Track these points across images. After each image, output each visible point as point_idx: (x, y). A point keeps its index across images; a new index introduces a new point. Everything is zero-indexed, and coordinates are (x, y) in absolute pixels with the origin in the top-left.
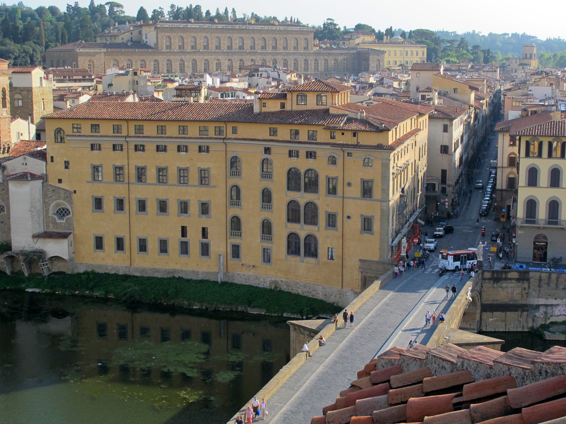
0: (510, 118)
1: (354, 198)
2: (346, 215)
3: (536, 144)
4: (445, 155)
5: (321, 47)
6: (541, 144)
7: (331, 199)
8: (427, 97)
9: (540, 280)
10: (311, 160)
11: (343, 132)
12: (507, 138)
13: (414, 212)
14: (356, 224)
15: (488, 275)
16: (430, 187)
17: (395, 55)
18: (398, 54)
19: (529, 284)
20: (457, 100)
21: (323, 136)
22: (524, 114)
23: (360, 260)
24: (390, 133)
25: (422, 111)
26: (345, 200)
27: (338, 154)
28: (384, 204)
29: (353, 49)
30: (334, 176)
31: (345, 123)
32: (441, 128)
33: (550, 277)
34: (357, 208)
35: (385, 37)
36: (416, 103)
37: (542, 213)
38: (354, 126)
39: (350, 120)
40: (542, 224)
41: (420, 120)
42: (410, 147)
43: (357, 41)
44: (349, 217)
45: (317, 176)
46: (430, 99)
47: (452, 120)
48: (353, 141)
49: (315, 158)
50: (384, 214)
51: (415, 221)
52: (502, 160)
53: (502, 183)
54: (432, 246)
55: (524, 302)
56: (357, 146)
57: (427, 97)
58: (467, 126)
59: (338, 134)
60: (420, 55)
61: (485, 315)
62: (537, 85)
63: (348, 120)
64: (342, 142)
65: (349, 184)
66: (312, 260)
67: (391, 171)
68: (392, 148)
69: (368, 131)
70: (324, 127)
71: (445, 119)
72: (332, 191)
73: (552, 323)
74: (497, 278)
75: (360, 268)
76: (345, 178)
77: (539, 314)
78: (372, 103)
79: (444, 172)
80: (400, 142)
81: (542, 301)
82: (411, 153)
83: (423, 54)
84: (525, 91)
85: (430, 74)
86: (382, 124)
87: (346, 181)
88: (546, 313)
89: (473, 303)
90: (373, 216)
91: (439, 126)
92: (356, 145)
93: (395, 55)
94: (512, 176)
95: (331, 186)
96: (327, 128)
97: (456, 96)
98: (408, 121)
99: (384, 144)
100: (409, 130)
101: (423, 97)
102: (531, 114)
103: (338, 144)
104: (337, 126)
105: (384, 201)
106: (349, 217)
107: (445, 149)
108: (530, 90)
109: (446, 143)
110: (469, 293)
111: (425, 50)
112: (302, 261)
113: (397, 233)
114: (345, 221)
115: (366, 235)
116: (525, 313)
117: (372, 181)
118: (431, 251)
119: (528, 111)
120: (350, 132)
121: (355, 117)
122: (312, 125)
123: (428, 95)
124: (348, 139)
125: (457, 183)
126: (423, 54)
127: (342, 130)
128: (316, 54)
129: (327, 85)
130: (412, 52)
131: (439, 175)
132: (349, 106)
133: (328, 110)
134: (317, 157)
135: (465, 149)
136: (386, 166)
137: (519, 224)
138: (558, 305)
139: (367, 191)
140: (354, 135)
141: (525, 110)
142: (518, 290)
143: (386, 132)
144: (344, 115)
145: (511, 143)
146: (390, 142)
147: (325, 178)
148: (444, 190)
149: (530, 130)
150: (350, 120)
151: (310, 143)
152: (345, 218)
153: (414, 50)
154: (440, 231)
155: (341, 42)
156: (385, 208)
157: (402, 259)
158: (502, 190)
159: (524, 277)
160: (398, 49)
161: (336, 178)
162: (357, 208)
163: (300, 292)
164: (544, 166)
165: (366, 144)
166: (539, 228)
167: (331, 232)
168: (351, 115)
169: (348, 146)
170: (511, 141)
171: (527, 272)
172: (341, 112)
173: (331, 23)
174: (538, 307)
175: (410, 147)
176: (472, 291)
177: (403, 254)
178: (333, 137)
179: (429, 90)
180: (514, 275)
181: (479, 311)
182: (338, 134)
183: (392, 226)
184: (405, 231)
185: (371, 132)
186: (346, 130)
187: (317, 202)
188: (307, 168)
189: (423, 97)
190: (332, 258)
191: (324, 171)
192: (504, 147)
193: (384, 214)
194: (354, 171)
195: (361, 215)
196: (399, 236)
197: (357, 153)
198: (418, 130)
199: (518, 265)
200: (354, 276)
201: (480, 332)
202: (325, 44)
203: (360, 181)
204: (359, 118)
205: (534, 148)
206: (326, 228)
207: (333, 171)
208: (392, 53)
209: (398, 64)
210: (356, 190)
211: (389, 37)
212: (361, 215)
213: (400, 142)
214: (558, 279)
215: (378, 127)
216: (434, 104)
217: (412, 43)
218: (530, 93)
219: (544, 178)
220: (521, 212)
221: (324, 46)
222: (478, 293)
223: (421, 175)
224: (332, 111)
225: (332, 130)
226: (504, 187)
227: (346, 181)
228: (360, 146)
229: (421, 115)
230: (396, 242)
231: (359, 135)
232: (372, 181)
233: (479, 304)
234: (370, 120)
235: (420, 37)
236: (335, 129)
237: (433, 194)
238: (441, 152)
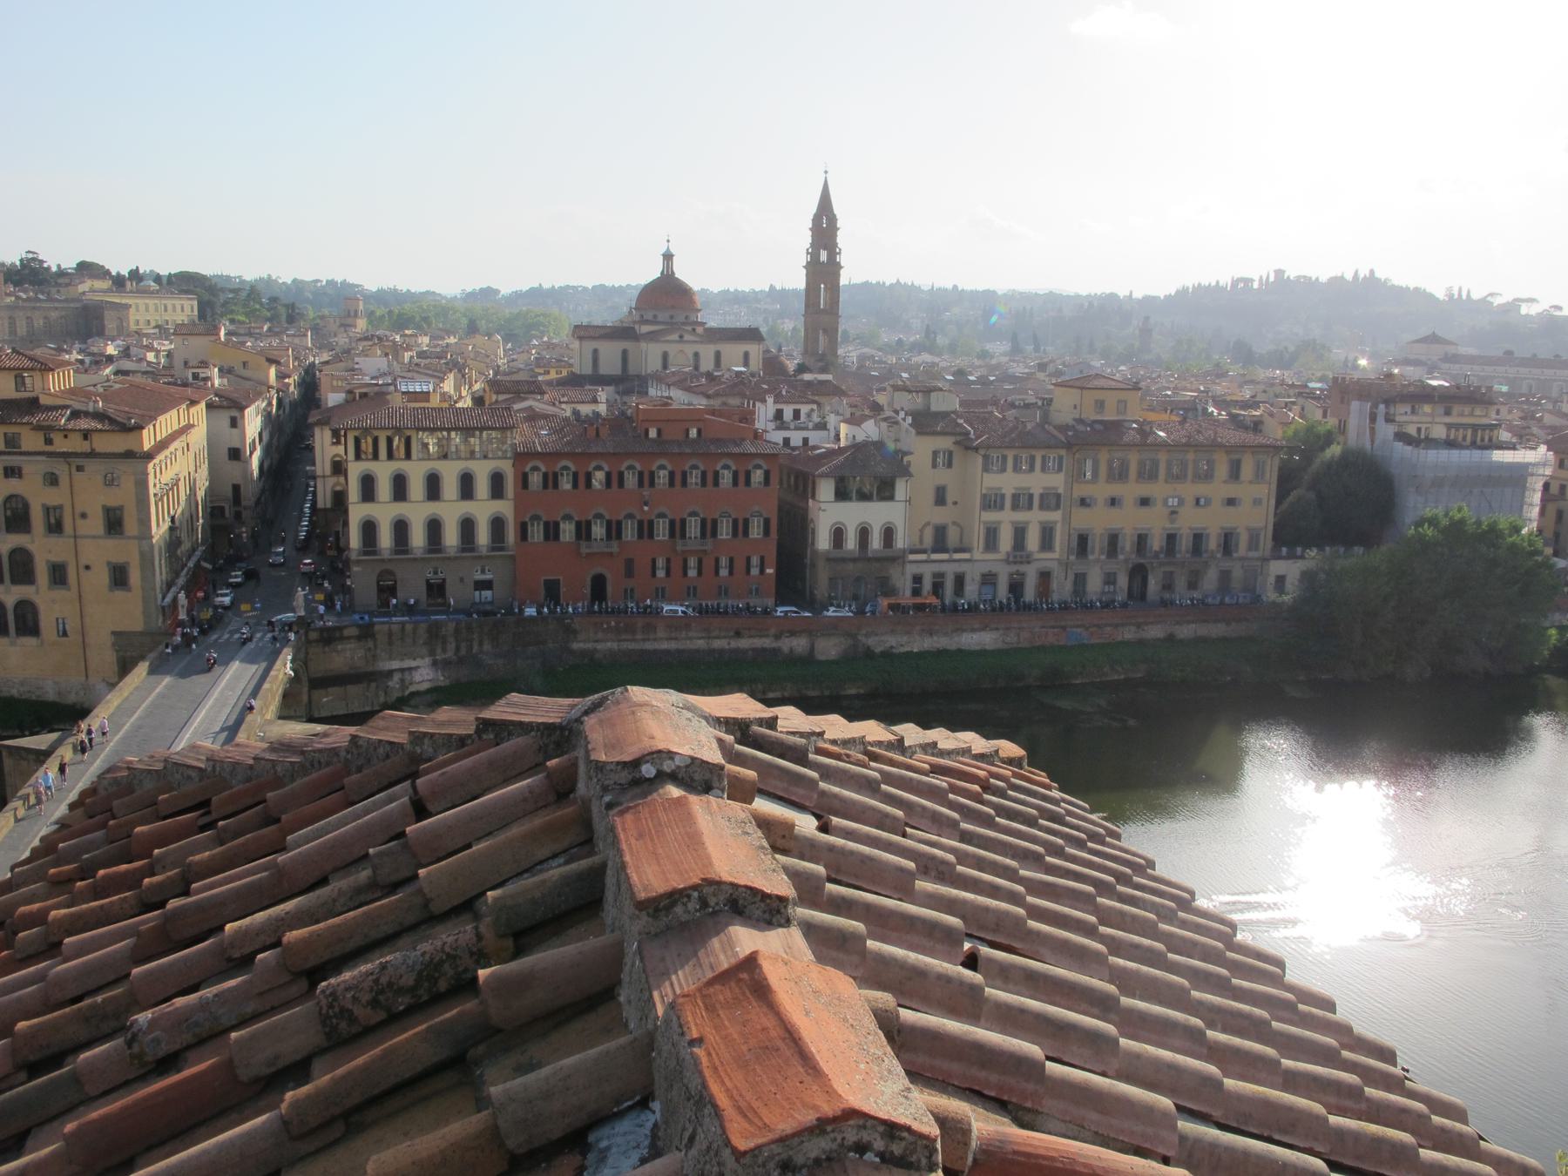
0: (331, 404)
1: (94, 537)
2: (83, 562)
3: (370, 440)
5: (18, 298)
6: (376, 441)
7: (53, 540)
9: (390, 634)
10: (14, 481)
12: (328, 434)
13: (194, 550)
14: (101, 577)
15: (313, 635)
16: (214, 512)
17: (147, 310)
18: (152, 308)
19: (375, 640)
21: (31, 441)
22: (350, 397)
23: (114, 633)
24: (145, 432)
25: (196, 397)
27: (61, 469)
29: (73, 300)
31: (69, 420)
32: (227, 422)
33: (403, 629)
34: (99, 552)
35: (128, 284)
36: (185, 385)
37: (385, 539)
38: (84, 424)
39: (76, 414)
40: (386, 555)
41: (193, 410)
42: (179, 453)
43: (82, 288)
44: (87, 567)
45: (26, 506)
46: (206, 379)
47: (242, 409)
48: (84, 447)
49: (20, 476)
50: (146, 560)
51: (197, 565)
52: (322, 465)
53: (324, 501)
54: (227, 600)
55: (370, 669)
56: (92, 454)
58: (268, 417)
60: (188, 310)
61: (316, 694)
65: (84, 516)
66: (30, 641)
67: (152, 491)
68: (149, 456)
72: (55, 528)
73: (413, 694)
74: (329, 638)
75: (113, 645)
77: (394, 682)
79: (236, 488)
80: (162, 445)
81: (395, 665)
82: (180, 462)
84: (350, 364)
87: (78, 510)
88: (402, 680)
89: (294, 681)
91: (224, 418)
93: (147, 310)
94: (338, 488)
95: (53, 521)
96: (38, 428)
97: (245, 373)
98: (174, 412)
100: (176, 427)
101: (195, 376)
106: (87, 567)
107: (235, 454)
109: (236, 445)
110: (289, 665)
112: (13, 644)
113: (169, 585)
115: (119, 594)
116: (373, 685)
117: (121, 508)
118: (226, 608)
123: (203, 373)
124: (75, 444)
125: (258, 502)
128: (9, 307)
129: (31, 359)
131: (229, 493)
132: (72, 392)
135: (267, 451)
136: (142, 484)
137: (353, 556)
138: (417, 668)
139: (113, 523)
140: (85, 438)
141: (350, 392)
142: (361, 653)
144: (66, 407)
146: (147, 447)
148: (238, 515)
150: (76, 414)
151: (9, 453)
152: (82, 570)
153: (178, 303)
154: (237, 577)
155: (54, 290)
157: (181, 624)
158: (325, 510)
159: (366, 633)
160: (151, 302)
161: (61, 507)
162: (99, 552)
163: (14, 692)
164: (383, 471)
166: (383, 561)
167: (59, 593)
168: (77, 406)
171: (371, 625)
173: (34, 259)
174: (390, 673)
175: (179, 453)
176: (292, 661)
177: (183, 616)
178: (49, 442)
179: (204, 364)
180: (353, 631)
181: (305, 689)
182: (57, 438)
183: (161, 573)
184: (181, 581)
185: (111, 435)
187: (30, 547)
188: (7, 493)
189: (195, 376)
190: (65, 634)
191: (38, 497)
192: (325, 447)
193: (146, 560)
194: (90, 495)
196: (174, 589)
197: (92, 466)
198: (189, 427)
199: (357, 617)
200: (104, 656)
201: (311, 720)
202: (25, 291)
205: (367, 445)
207: (54, 497)
208: (142, 308)
209: (153, 324)
210: (96, 524)
212: (109, 563)
213: (162, 445)
214: (415, 630)
219: (384, 489)
220: (355, 540)
221: (24, 296)
222: (300, 663)
223: (200, 494)
224: (44, 400)
225: (47, 431)
226: (329, 506)
227: (78, 510)
229: (193, 403)
230: (168, 599)
232: (121, 508)
233: (305, 679)
235: (185, 283)
236: (51, 428)
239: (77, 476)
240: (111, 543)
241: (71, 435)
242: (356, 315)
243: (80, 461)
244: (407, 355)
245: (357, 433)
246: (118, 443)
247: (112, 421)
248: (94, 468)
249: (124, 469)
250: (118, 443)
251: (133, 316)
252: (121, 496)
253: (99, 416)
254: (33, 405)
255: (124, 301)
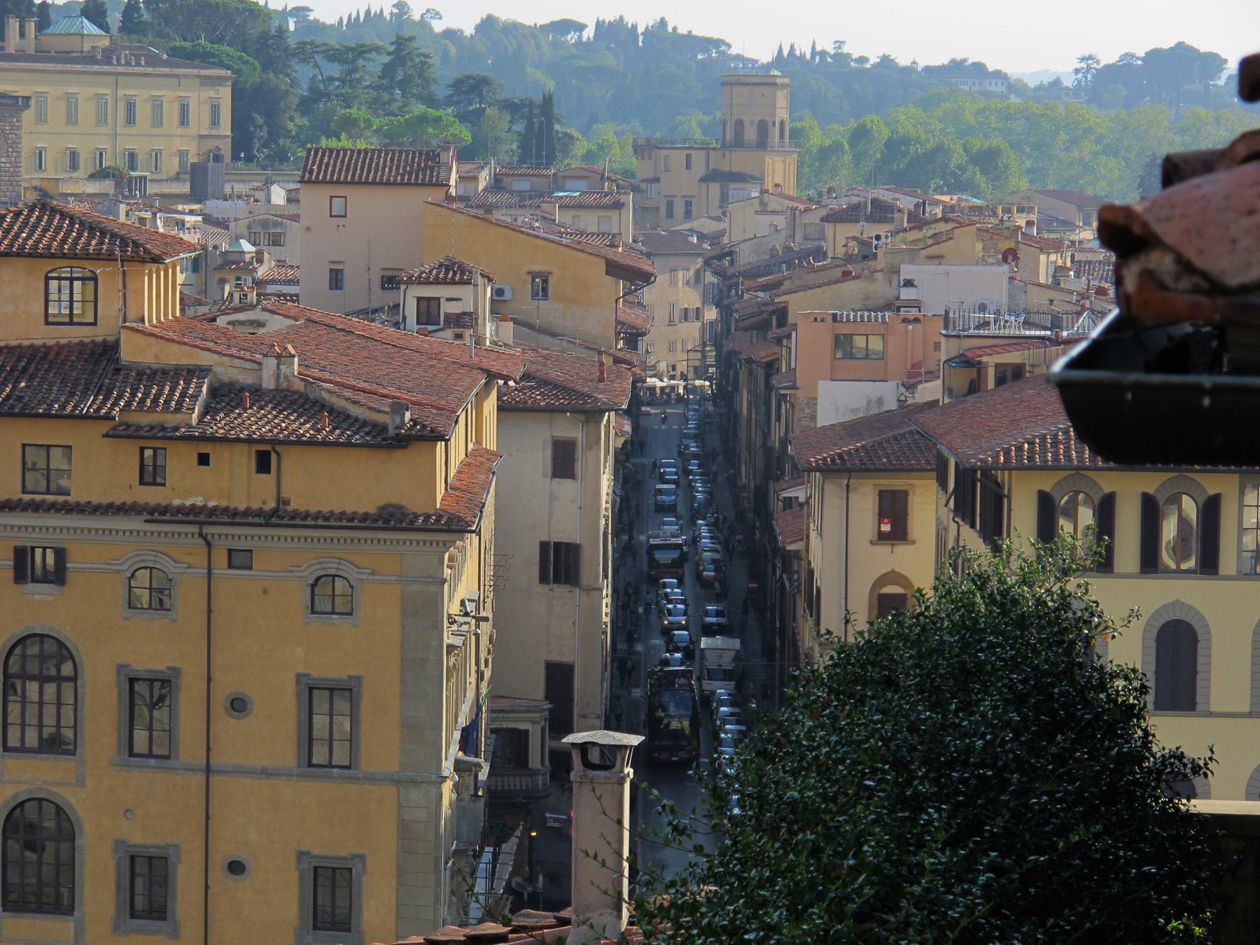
0: (826, 417)
1: (265, 773)
2: (223, 852)
4: (561, 590)
6: (1106, 510)
8: (447, 308)
10: (38, 593)
11: (204, 448)
12: (865, 502)
17: (71, 118)
18: (86, 110)
20: (554, 335)
21: (98, 469)
22: (962, 379)
26: (215, 779)
27: (181, 555)
28: (415, 795)
30: (159, 666)
31: (207, 410)
32: (542, 458)
38: (256, 422)
44: (236, 867)
46: (461, 321)
48: (257, 492)
56: (279, 516)
57: (447, 308)
59: (179, 465)
60: (200, 120)
62: (939, 258)
63: (214, 392)
64: (199, 501)
65: (238, 705)
69: (336, 444)
70: (105, 427)
71: (562, 410)
76: (216, 674)
78: (260, 324)
79: (559, 678)
83: (215, 122)
84: (882, 288)
85: (414, 200)
86: (399, 408)
90: (361, 858)
92: (274, 512)
93: (71, 118)
96: (125, 433)
97: (548, 311)
99: (414, 504)
101: (428, 313)
102: (1000, 381)
103: (180, 510)
104: (171, 419)
105: (415, 783)
106: (236, 867)
108: (909, 283)
111: (224, 95)
114: (215, 889)
119: (980, 368)
120: (245, 447)
121: (247, 379)
122: (47, 415)
123: (455, 299)
124: (232, 482)
126: (215, 122)
127: (203, 438)
130: (158, 105)
133: (106, 352)
134: (70, 576)
140: (263, 464)
141: (966, 362)
143: (424, 446)
144: (194, 372)
145: (886, 528)
147: (110, 677)
149: (1055, 443)
150: (226, 396)
151: (35, 507)
152: (219, 874)
153: (169, 94)
156: (421, 815)
165: (325, 509)
168: (229, 370)
169: (233, 516)
170: (881, 516)
172: (176, 356)
178: (150, 475)
182: (179, 465)
186: (224, 440)
187: (72, 798)
188: (20, 632)
189: (428, 313)
194: (265, 637)
195: (301, 855)
197: (274, 548)
203: (290, 688)
204: (268, 383)
206: (117, 927)
208: (57, 110)
210: (269, 734)
211: (31, 27)
212: (301, 855)
215: (384, 429)
216: (479, 341)
217: (154, 61)
218: (907, 294)
224: (132, 352)
227: (222, 694)
228: (294, 515)
231: (286, 463)
234: (326, 392)
236: (163, 434)
237: (517, 783)
238: (544, 579)
239: (229, 580)
240: (312, 791)
241: (218, 455)
242: (762, 144)
243: (241, 537)
244: (1045, 264)
245: (1047, 483)
246: (357, 483)
247: (341, 418)
248: (285, 561)
249: (375, 565)
250: (357, 483)
251: (34, 134)
252: (357, 646)
253: (285, 399)
254: (101, 360)
255: (20, 90)
